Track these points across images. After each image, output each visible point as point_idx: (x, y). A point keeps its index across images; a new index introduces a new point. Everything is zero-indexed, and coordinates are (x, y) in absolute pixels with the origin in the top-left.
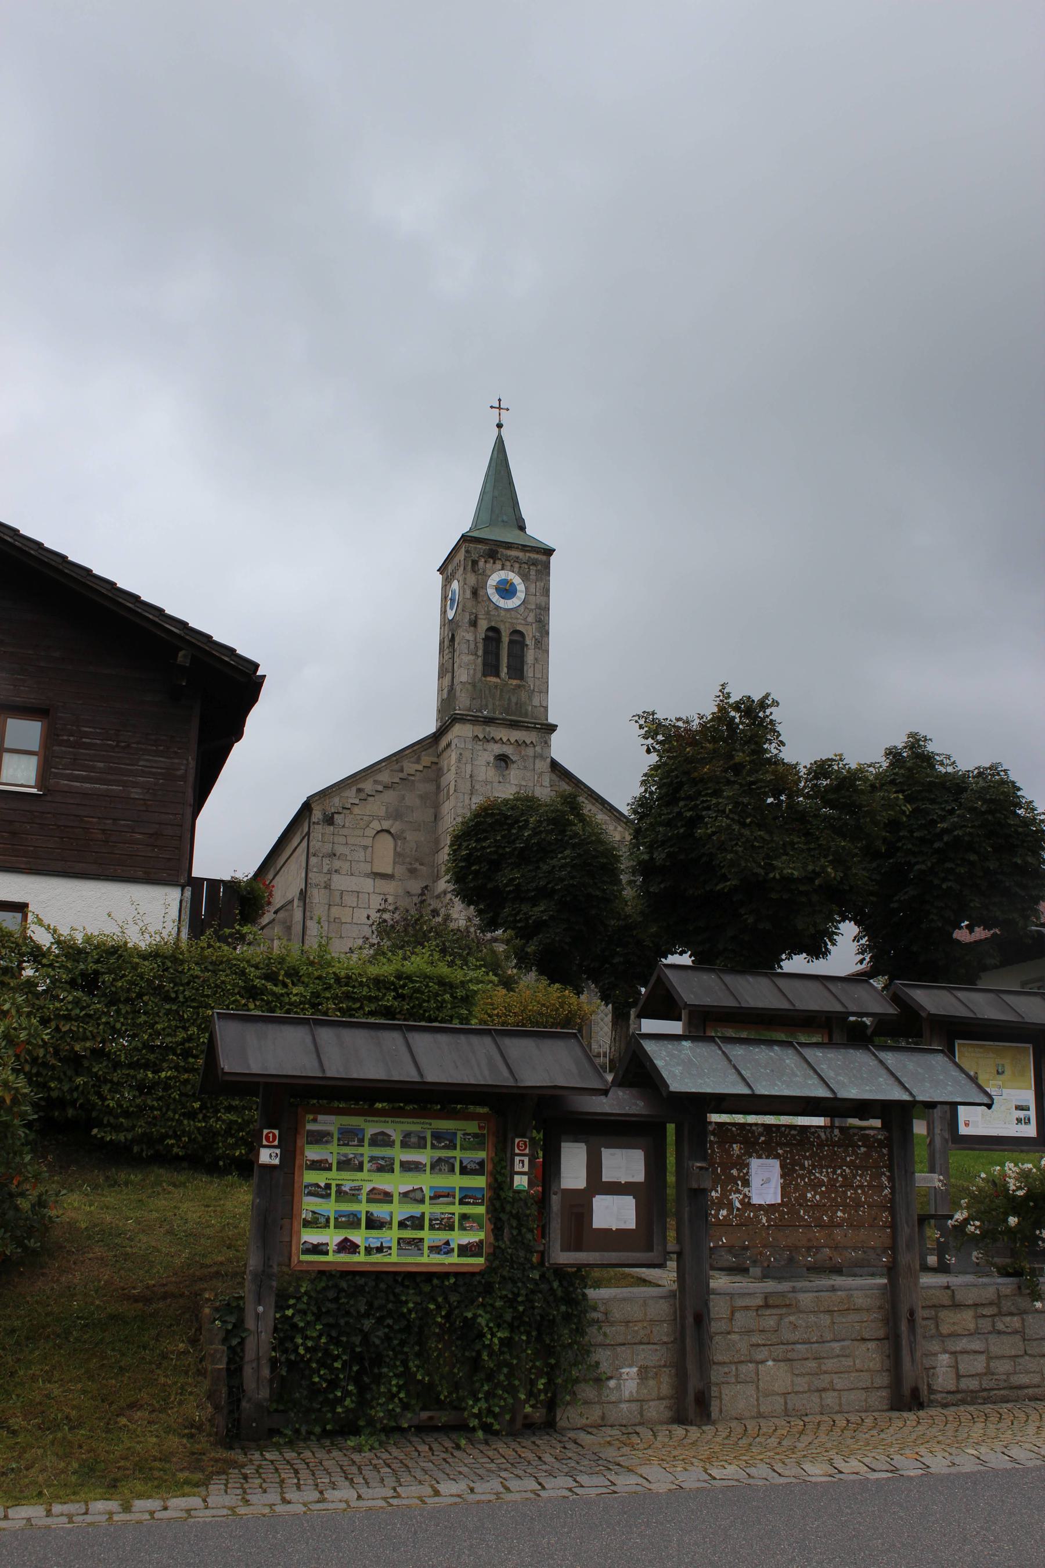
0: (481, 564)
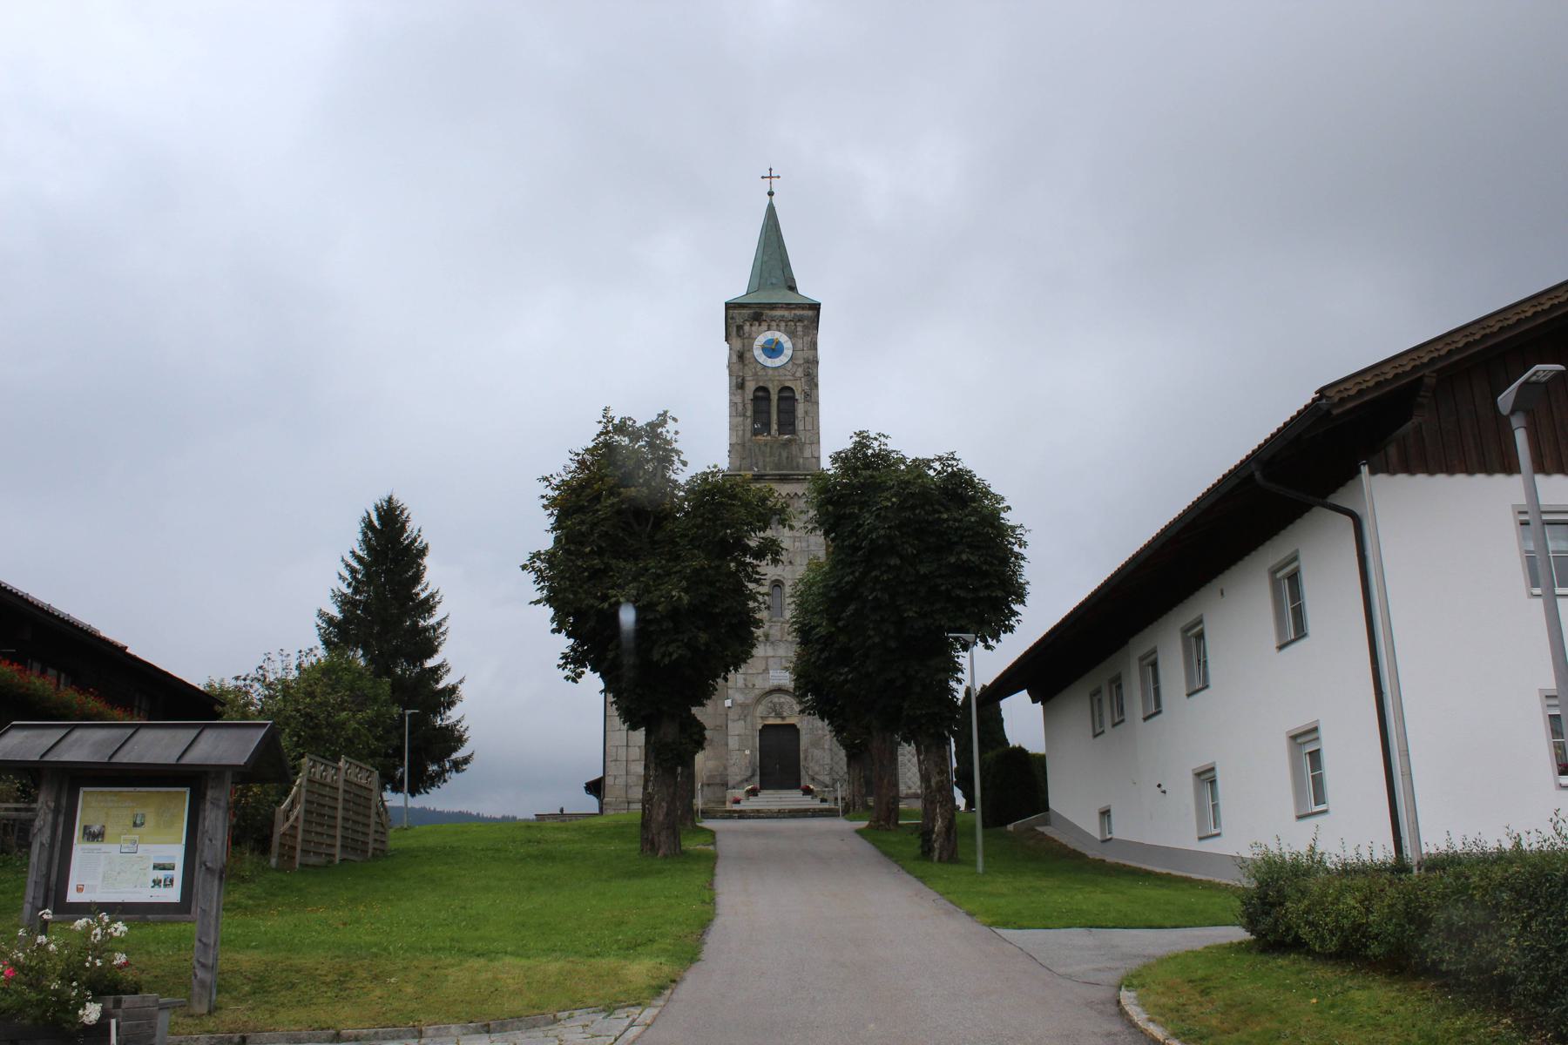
0: (747, 328)
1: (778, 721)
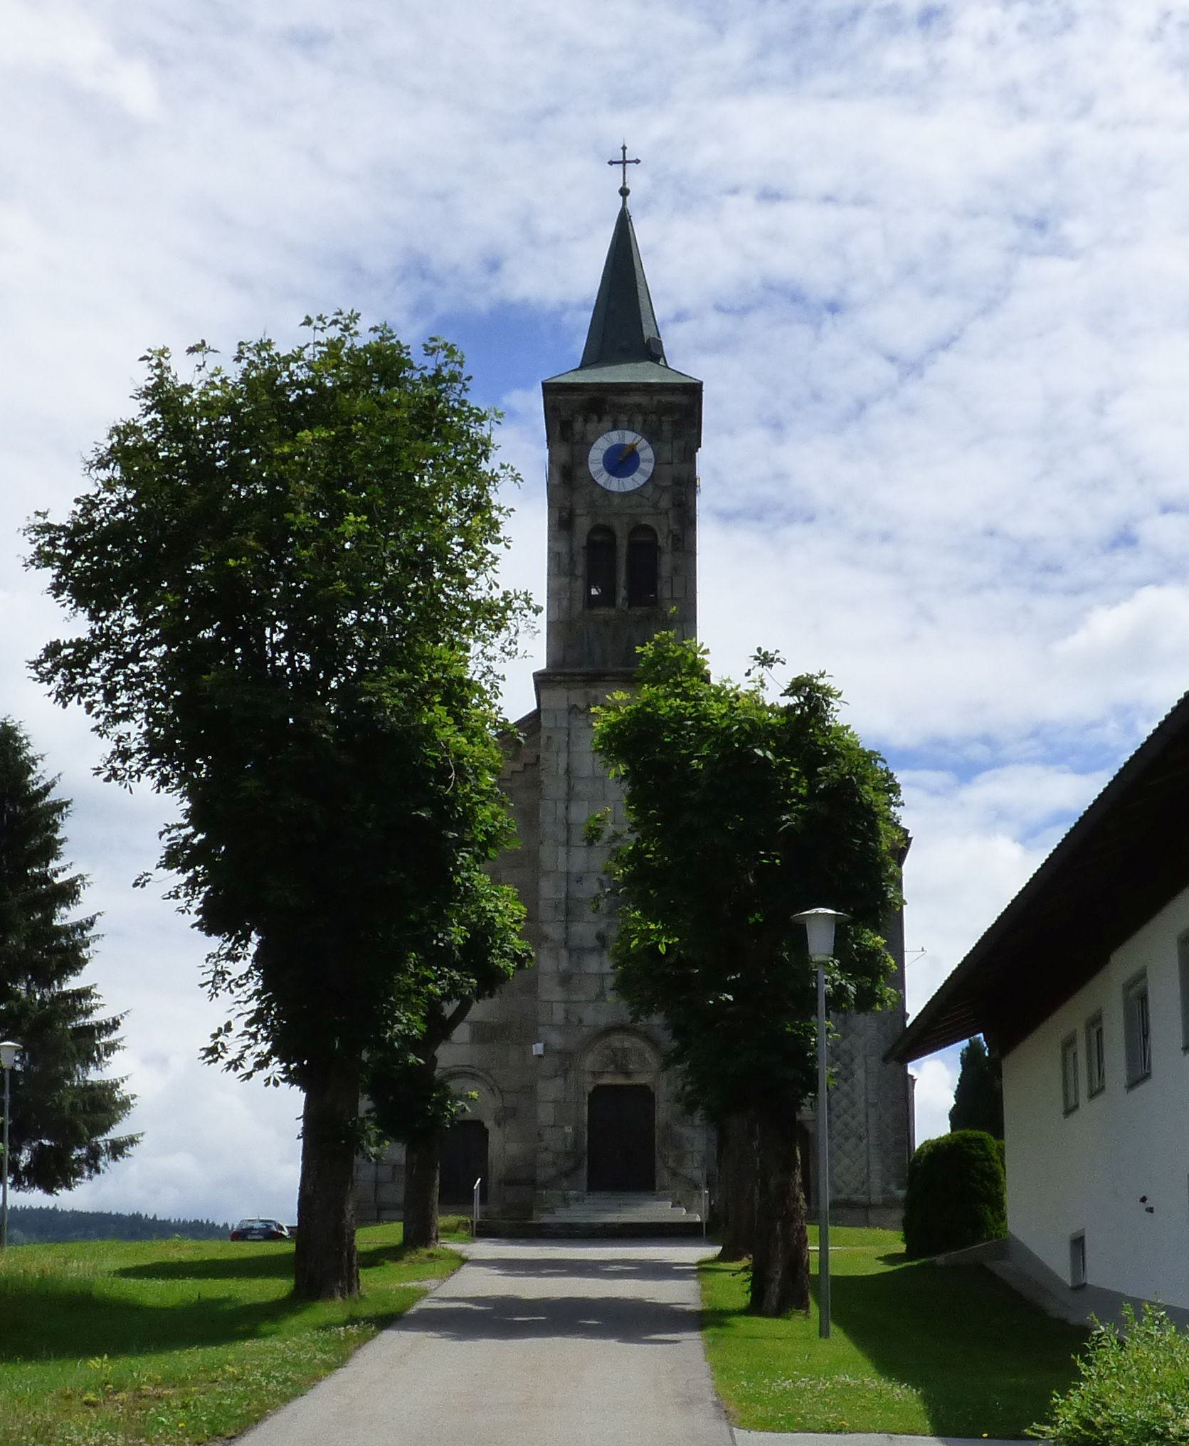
0: (578, 426)
1: (620, 1081)
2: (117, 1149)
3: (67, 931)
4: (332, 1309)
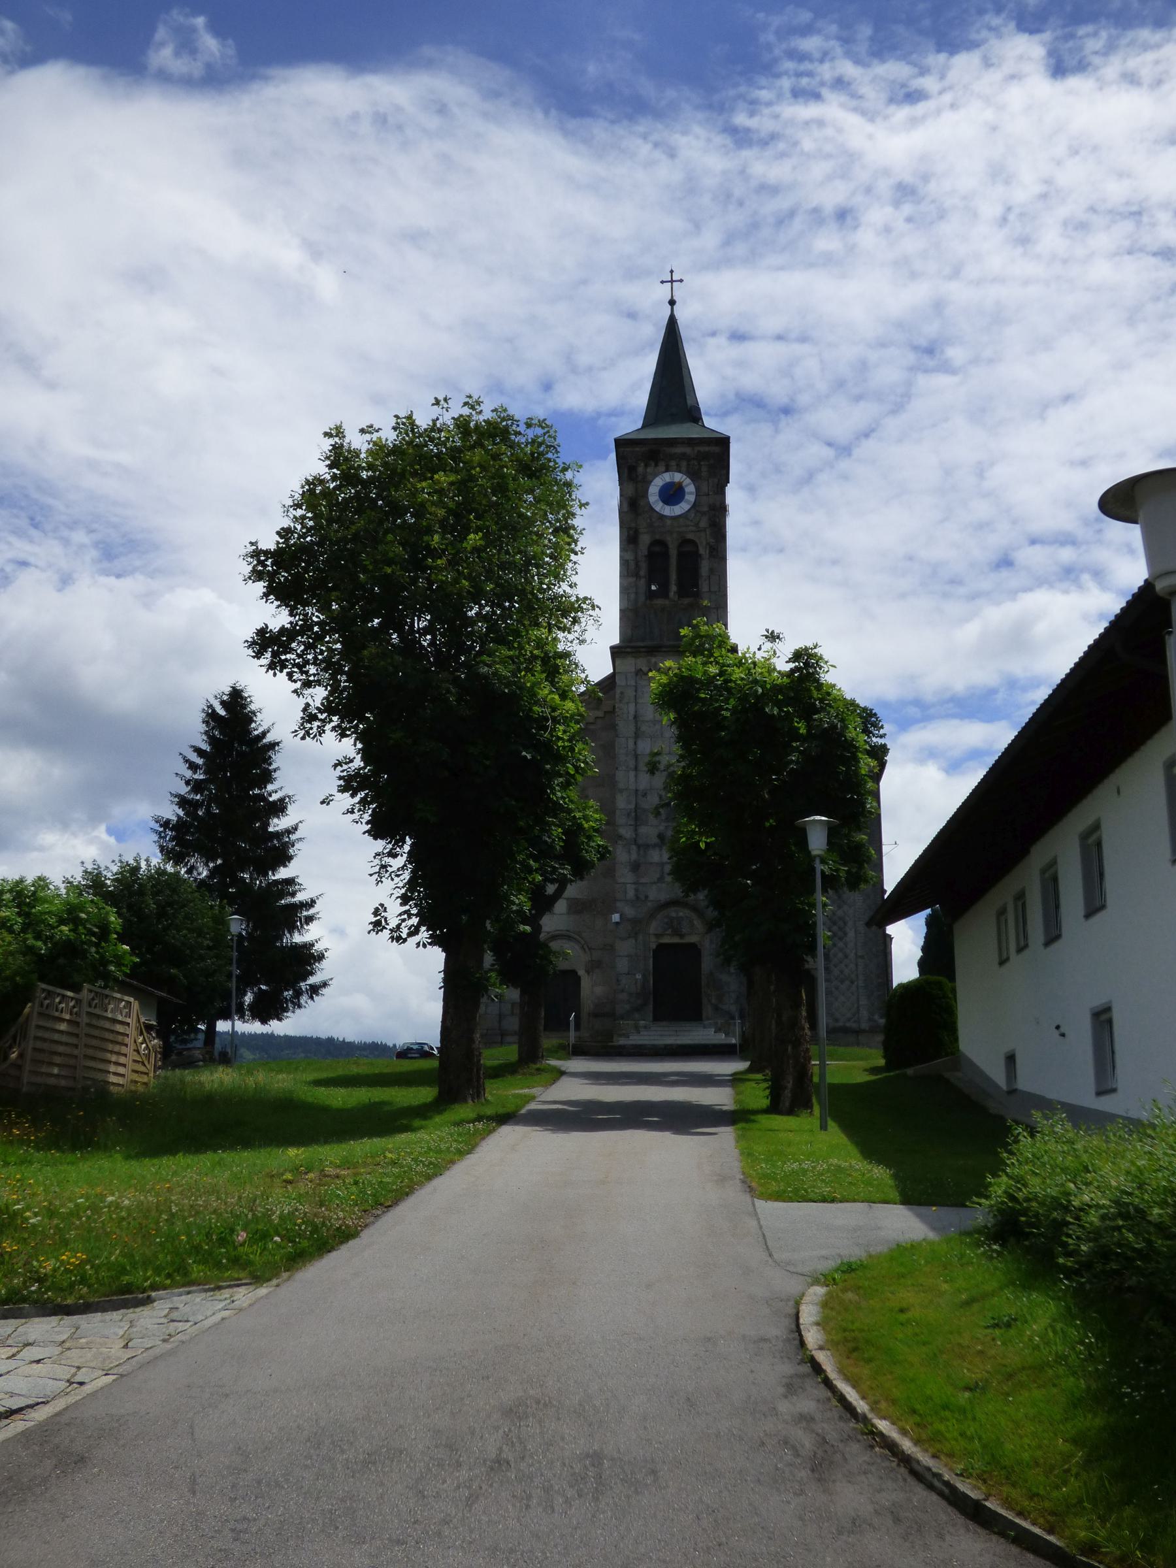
0: (641, 469)
1: (676, 940)
2: (314, 990)
3: (278, 835)
4: (465, 1111)
